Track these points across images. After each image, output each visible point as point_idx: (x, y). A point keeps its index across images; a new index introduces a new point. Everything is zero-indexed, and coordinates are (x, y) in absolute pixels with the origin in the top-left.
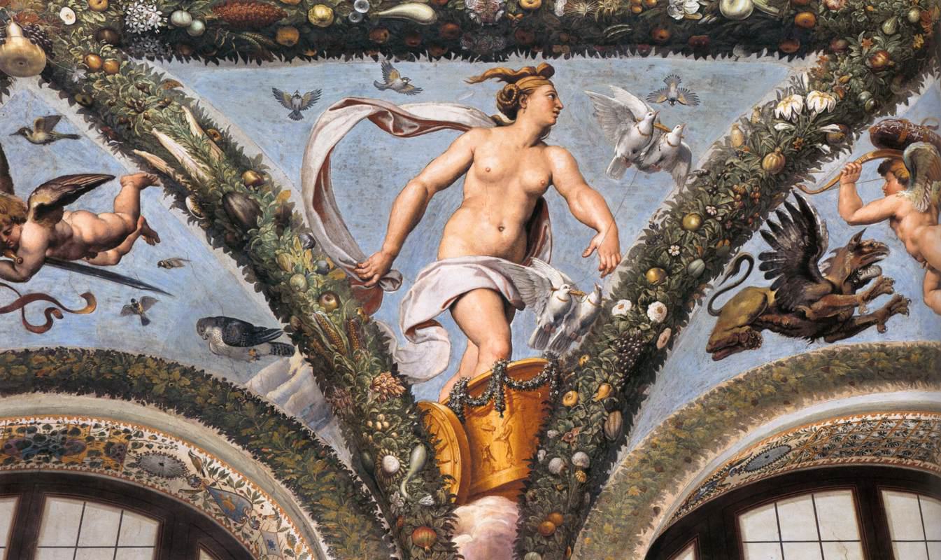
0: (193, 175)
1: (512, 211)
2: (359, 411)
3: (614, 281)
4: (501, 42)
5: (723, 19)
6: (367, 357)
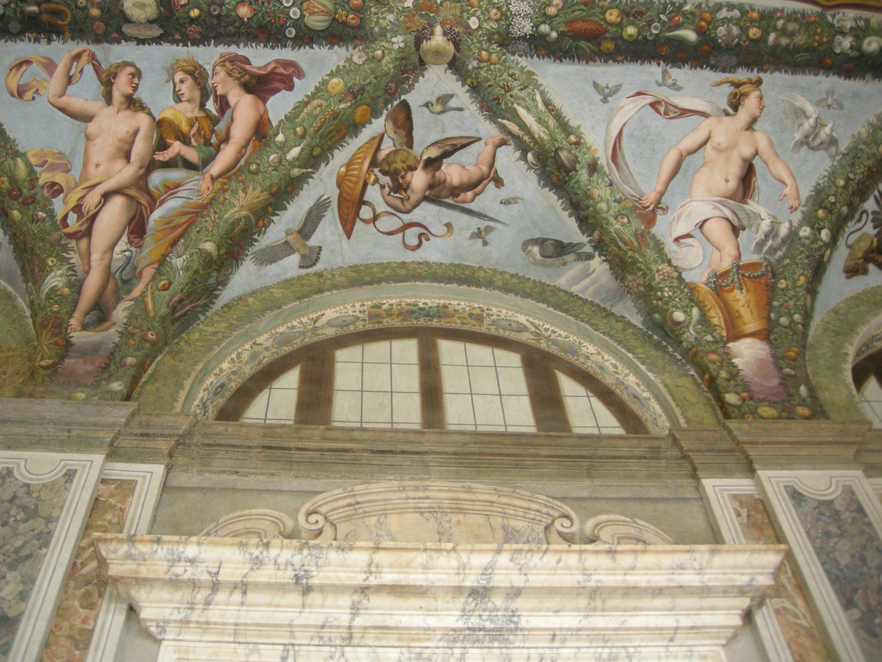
0: (536, 136)
1: (734, 171)
2: (650, 288)
3: (797, 217)
4: (734, 60)
5: (862, 55)
6: (651, 254)
